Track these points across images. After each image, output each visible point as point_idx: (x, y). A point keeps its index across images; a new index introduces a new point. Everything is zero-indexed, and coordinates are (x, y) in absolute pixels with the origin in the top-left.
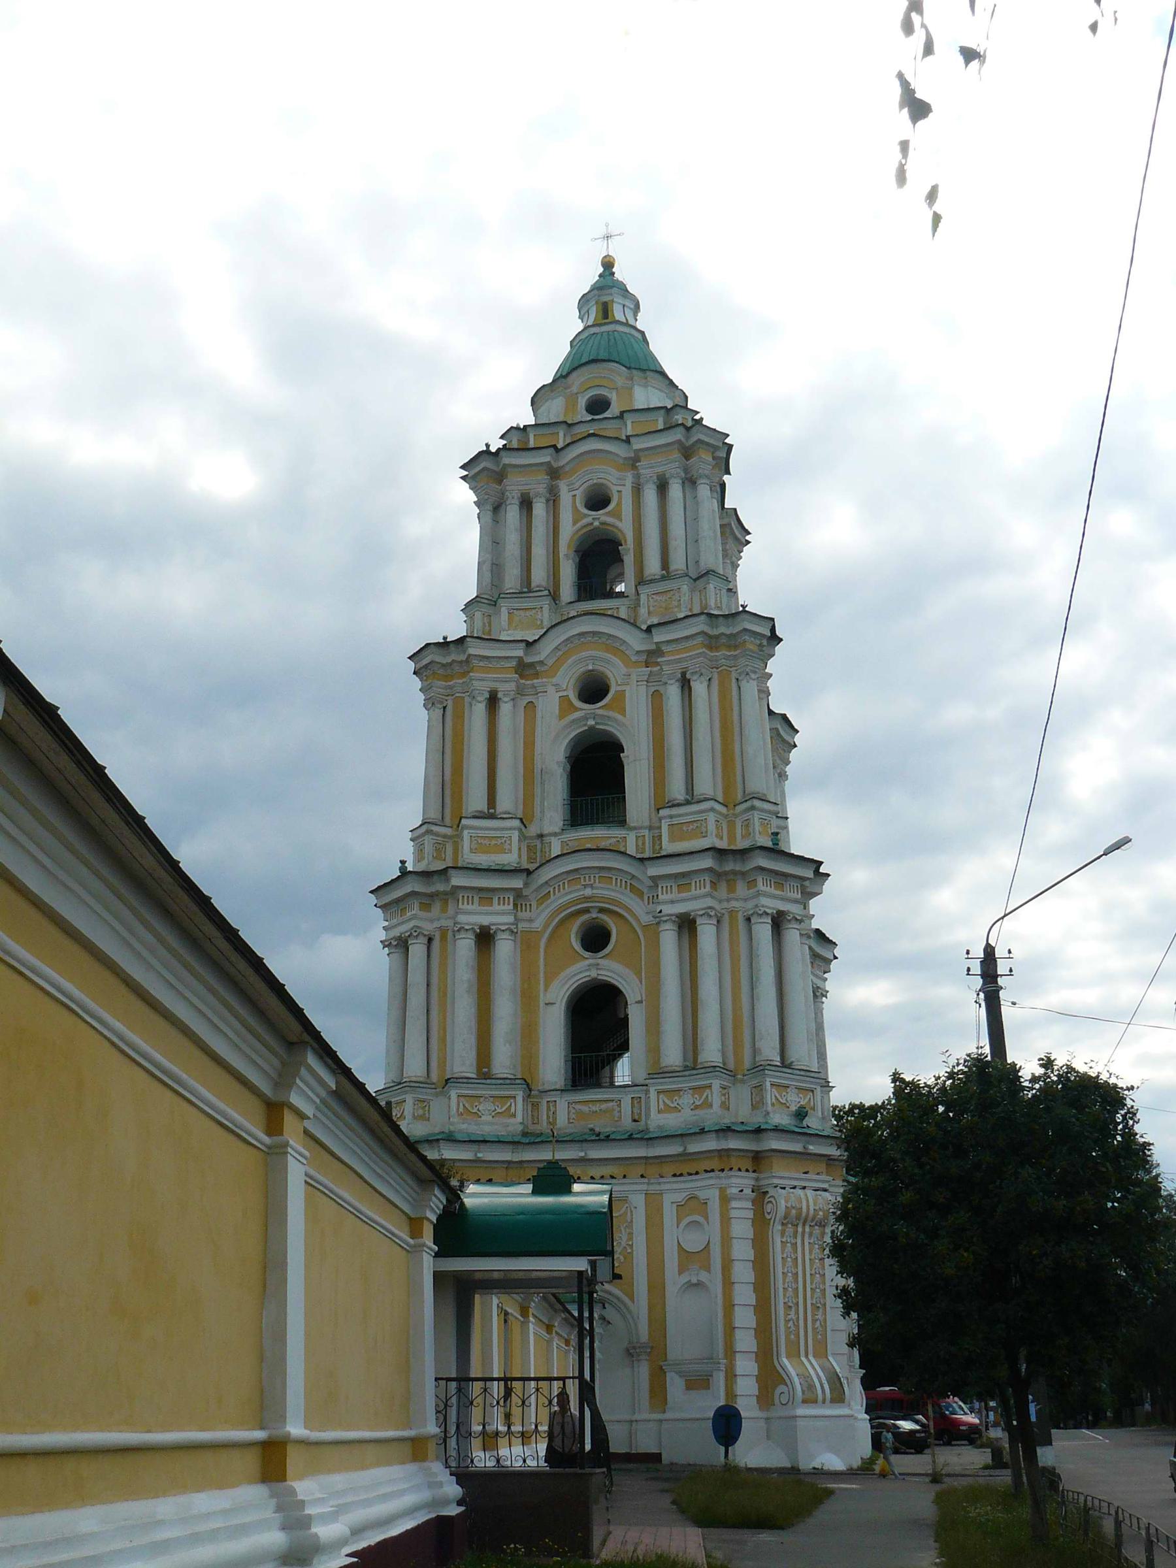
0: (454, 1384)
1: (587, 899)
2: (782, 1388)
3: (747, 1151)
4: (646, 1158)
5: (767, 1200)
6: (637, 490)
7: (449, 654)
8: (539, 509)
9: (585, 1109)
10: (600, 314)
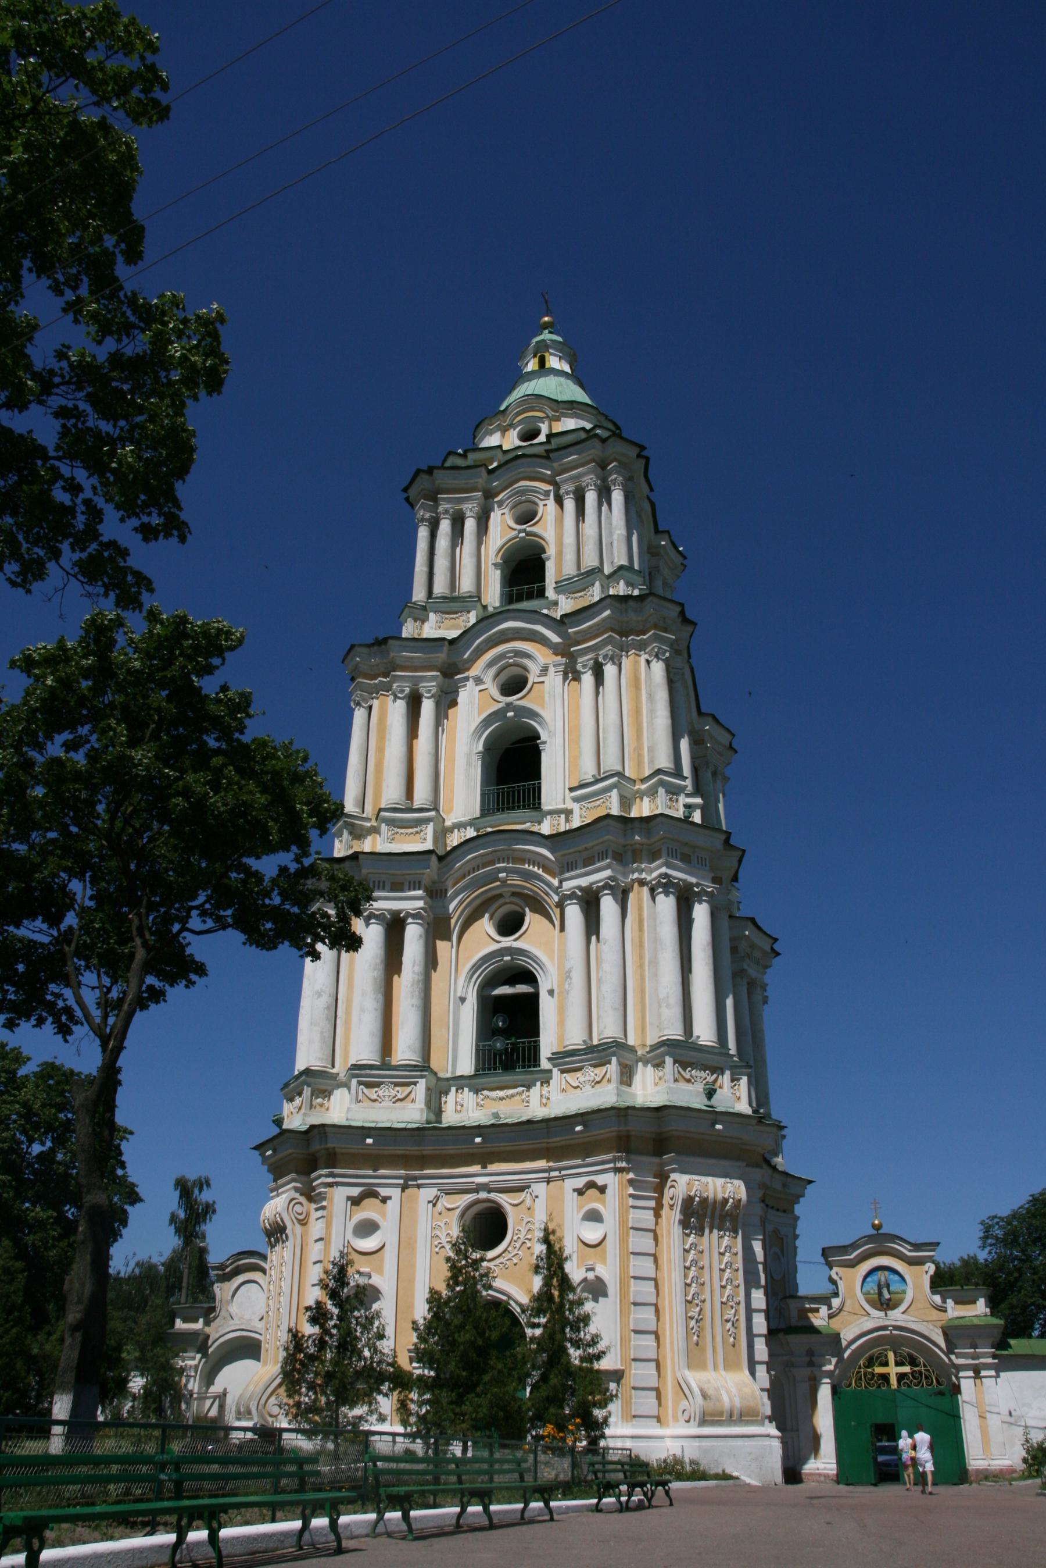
5: (669, 1184)
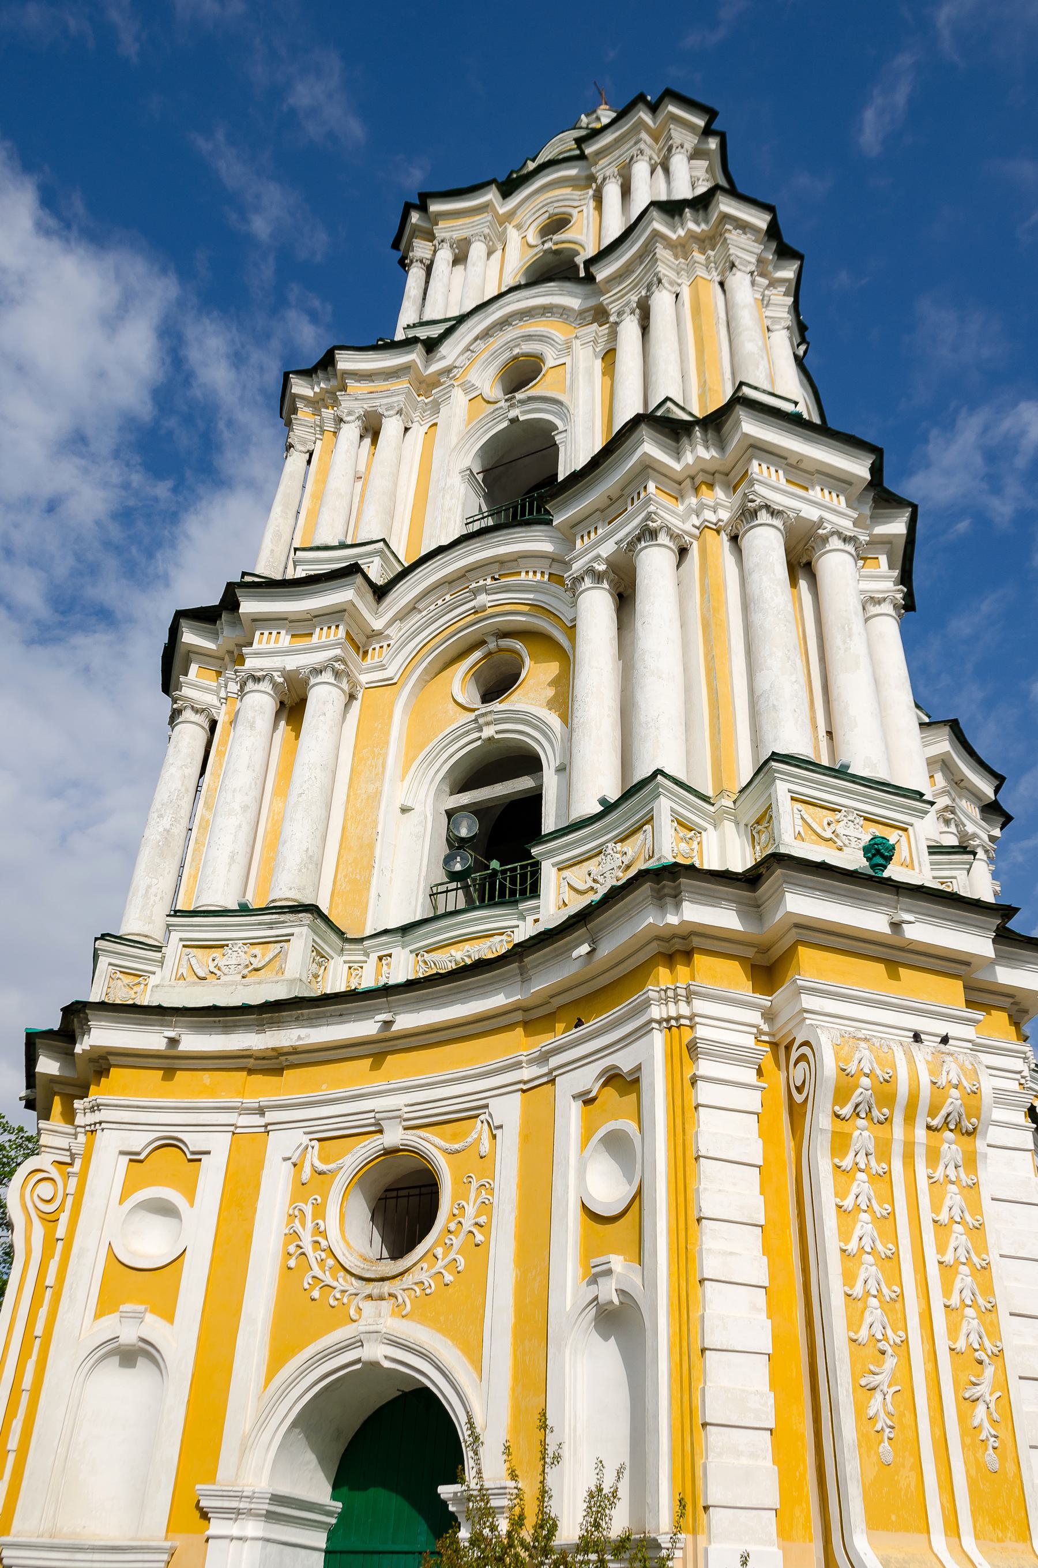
5: (794, 1055)
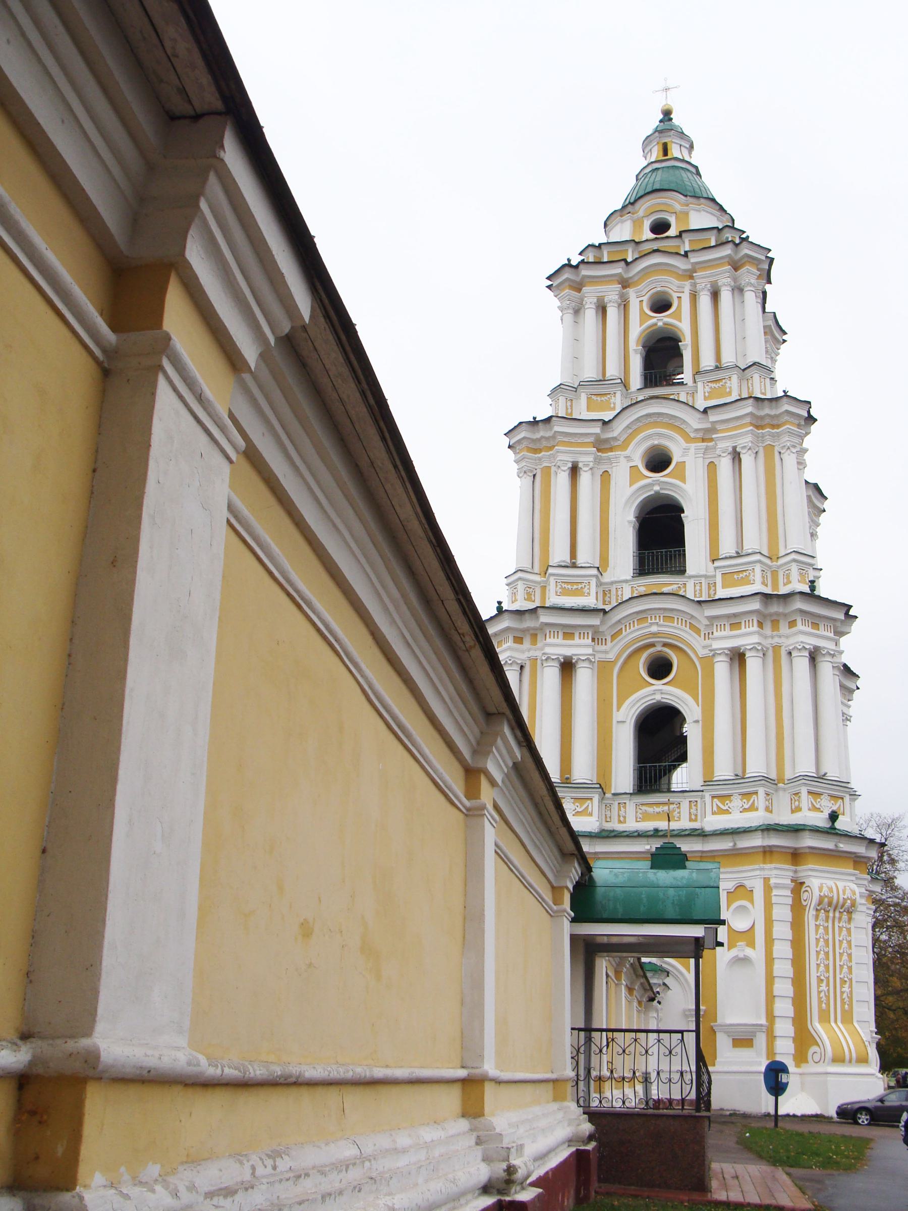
0: (582, 1034)
1: (654, 635)
2: (814, 1048)
3: (788, 848)
4: (703, 852)
6: (694, 297)
7: (538, 431)
8: (612, 313)
9: (650, 810)
10: (661, 153)
